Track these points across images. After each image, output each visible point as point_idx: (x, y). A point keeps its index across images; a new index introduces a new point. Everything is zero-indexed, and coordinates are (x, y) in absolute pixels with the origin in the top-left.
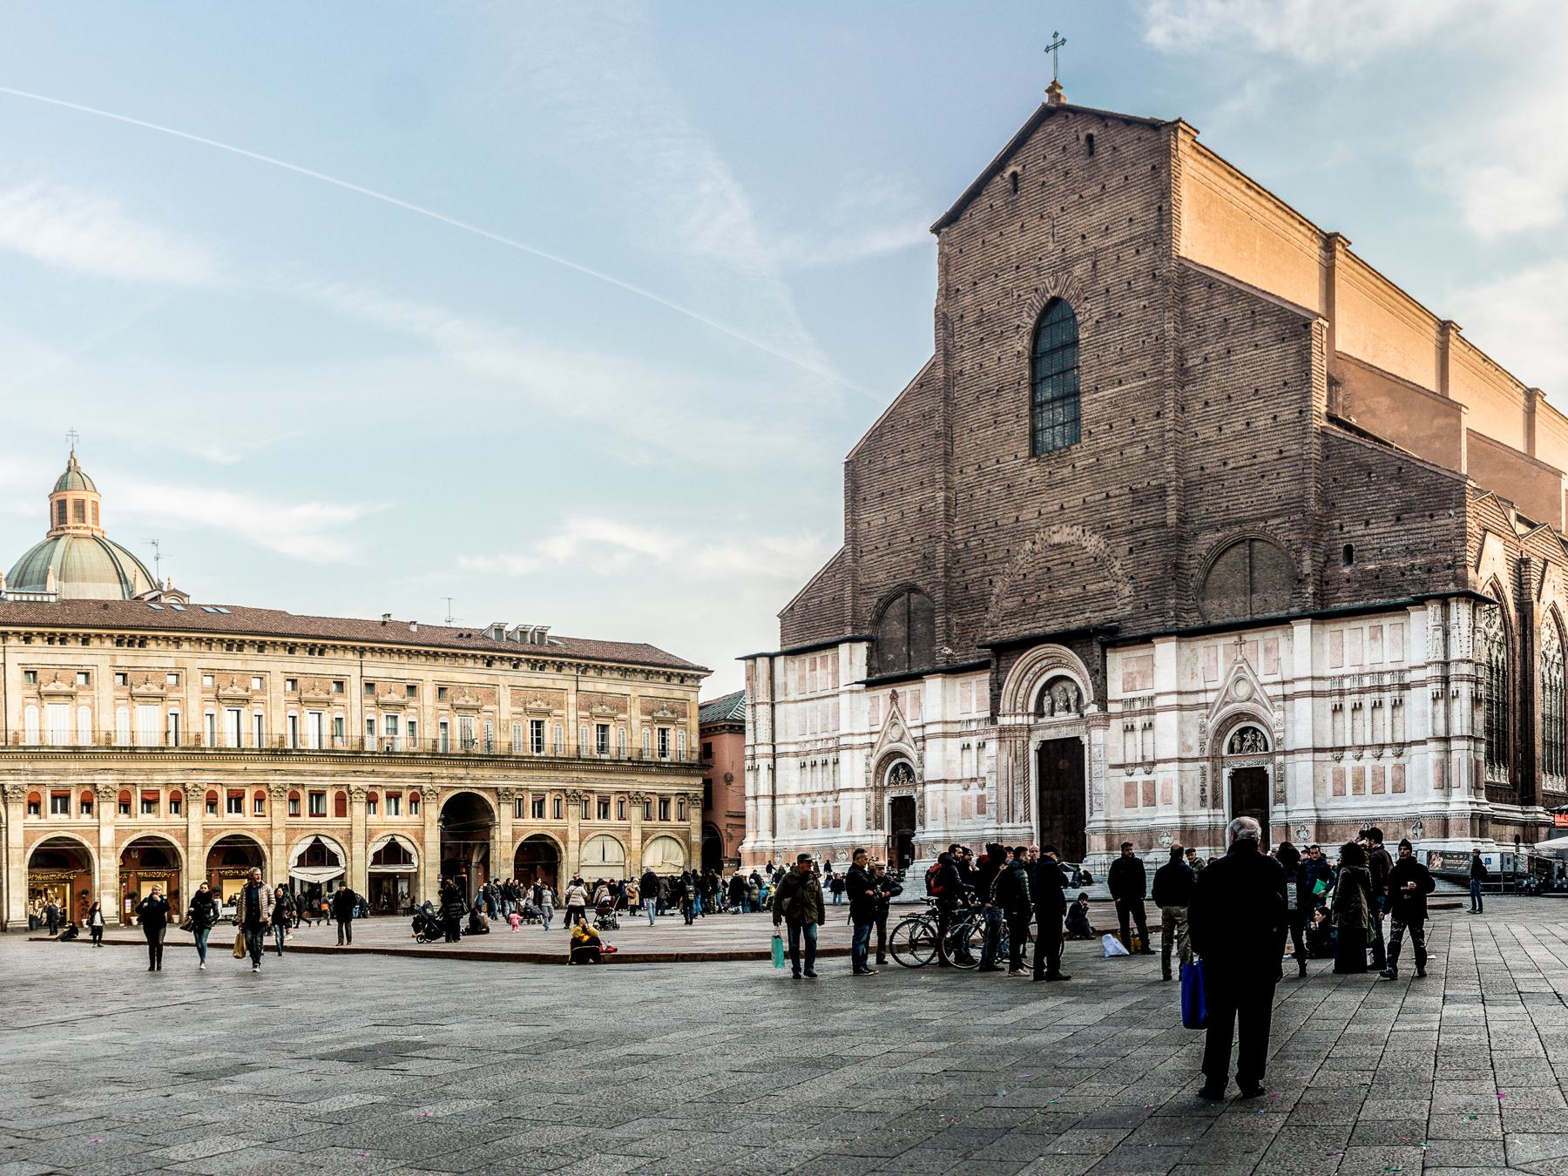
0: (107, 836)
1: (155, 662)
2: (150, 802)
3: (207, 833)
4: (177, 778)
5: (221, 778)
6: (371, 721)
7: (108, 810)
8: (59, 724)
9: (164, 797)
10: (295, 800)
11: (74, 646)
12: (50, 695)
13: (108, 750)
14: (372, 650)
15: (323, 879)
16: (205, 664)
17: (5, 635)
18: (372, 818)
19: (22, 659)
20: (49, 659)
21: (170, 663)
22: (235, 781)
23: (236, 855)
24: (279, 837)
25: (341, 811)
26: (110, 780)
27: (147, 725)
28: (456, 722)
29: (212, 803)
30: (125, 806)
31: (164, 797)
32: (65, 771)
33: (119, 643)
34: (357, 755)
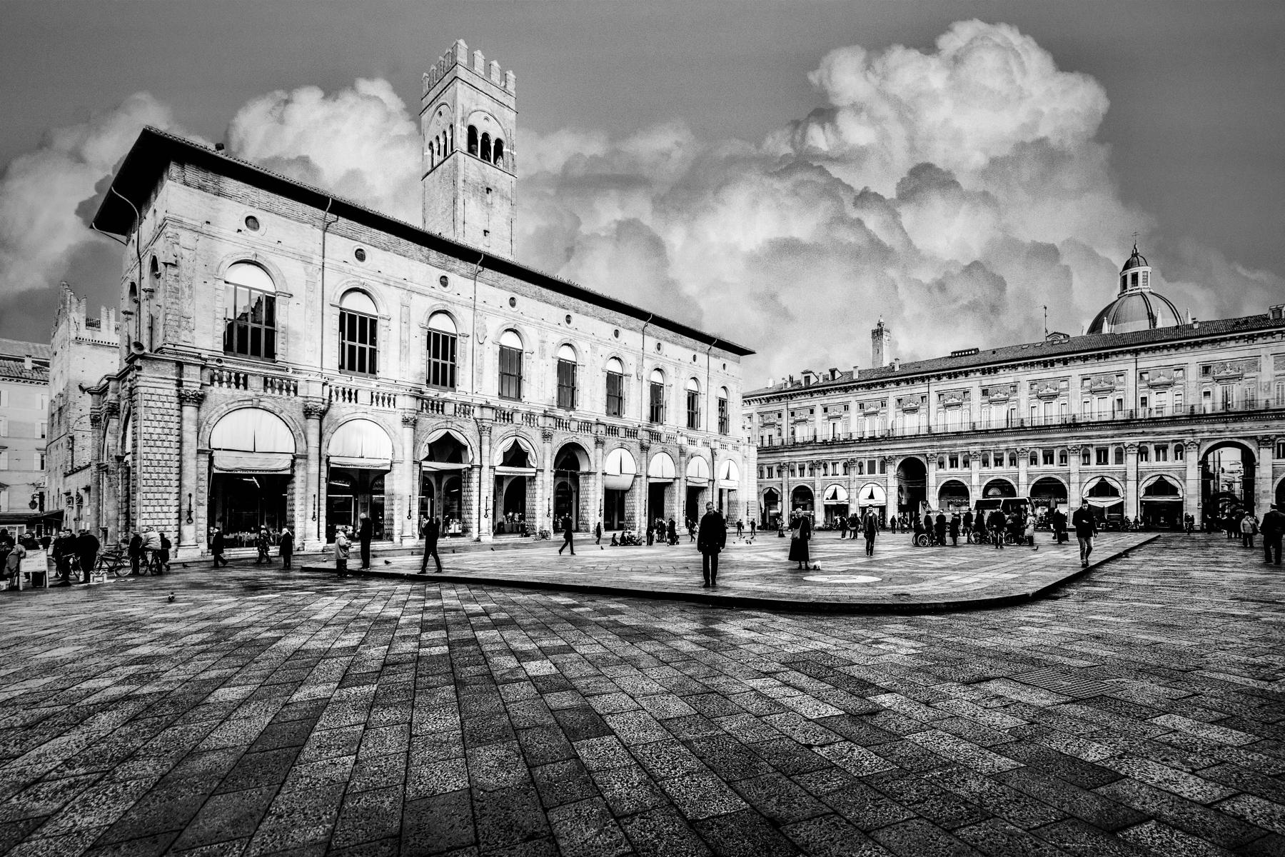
0: (976, 478)
1: (1002, 381)
2: (999, 462)
3: (1030, 476)
4: (1012, 445)
5: (1037, 443)
6: (1144, 399)
7: (976, 465)
8: (954, 420)
9: (1006, 457)
10: (1086, 455)
11: (961, 378)
12: (950, 406)
13: (975, 433)
14: (1143, 350)
15: (1107, 505)
16: (1030, 377)
17: (928, 378)
18: (1143, 464)
19: (937, 388)
20: (949, 387)
21: (1011, 380)
22: (1046, 444)
23: (1050, 489)
24: (1075, 478)
25: (1120, 458)
26: (977, 448)
27: (996, 417)
28: (1218, 390)
29: (1034, 460)
30: (985, 463)
31: (1006, 457)
32: (955, 445)
33: (983, 372)
34: (1130, 423)
